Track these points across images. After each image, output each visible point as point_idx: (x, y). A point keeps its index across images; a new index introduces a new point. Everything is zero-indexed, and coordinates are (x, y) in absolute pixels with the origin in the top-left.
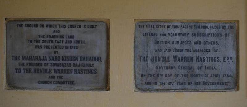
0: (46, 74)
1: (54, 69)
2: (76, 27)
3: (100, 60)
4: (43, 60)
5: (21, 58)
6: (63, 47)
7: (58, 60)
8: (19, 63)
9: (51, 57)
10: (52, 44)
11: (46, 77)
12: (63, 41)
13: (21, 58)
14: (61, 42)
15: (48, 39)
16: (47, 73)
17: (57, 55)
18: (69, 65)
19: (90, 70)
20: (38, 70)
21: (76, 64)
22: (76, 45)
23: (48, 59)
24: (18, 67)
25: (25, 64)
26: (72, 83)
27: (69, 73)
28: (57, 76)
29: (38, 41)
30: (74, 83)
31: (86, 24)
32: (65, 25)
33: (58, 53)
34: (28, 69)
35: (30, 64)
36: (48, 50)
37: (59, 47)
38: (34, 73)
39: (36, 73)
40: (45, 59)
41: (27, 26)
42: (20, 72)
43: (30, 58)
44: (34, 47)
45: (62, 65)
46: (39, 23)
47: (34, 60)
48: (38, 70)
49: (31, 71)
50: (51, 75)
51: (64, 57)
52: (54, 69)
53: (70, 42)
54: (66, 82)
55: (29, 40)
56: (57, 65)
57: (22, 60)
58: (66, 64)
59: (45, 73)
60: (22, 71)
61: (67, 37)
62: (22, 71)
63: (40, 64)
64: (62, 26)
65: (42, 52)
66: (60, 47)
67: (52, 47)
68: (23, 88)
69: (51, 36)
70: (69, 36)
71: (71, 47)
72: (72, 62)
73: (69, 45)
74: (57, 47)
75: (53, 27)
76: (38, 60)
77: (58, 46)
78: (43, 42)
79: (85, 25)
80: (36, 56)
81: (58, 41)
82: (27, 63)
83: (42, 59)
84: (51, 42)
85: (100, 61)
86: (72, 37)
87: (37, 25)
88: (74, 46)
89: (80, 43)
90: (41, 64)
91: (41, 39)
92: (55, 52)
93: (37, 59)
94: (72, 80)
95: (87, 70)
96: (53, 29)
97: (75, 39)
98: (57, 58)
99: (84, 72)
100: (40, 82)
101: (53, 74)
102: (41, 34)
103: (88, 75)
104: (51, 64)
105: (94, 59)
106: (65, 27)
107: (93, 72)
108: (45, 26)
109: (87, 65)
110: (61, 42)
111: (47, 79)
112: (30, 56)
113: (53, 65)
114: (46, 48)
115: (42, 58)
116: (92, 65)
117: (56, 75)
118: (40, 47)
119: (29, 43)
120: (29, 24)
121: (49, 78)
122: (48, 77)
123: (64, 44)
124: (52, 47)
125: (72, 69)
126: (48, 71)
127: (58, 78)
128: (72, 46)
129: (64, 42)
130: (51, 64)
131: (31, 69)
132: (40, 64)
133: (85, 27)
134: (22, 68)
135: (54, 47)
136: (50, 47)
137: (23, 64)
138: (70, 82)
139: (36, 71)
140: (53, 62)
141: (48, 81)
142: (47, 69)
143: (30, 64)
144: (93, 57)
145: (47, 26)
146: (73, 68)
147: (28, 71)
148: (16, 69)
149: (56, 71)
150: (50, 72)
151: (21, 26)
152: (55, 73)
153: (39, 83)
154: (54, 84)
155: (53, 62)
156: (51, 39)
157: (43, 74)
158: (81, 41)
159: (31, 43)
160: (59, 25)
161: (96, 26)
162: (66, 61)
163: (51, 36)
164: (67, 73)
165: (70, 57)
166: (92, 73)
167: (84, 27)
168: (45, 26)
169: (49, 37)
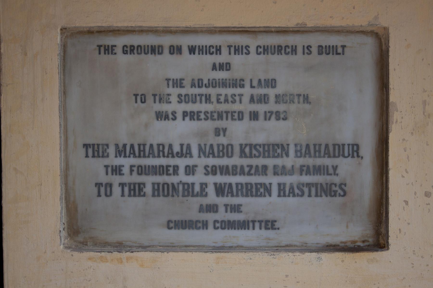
0: (190, 198)
1: (215, 184)
2: (283, 51)
3: (355, 154)
4: (180, 155)
5: (112, 150)
7: (228, 156)
8: (106, 167)
9: (205, 145)
10: (209, 107)
11: (190, 208)
12: (241, 95)
13: (112, 150)
14: (237, 98)
15: (196, 91)
16: (193, 196)
17: (223, 140)
18: (260, 169)
19: (325, 186)
20: (166, 186)
21: (284, 167)
22: (281, 107)
23: (195, 151)
24: (104, 179)
25: (126, 170)
26: (270, 226)
27: (261, 195)
28: (226, 206)
29: (162, 98)
30: (277, 225)
31: (315, 41)
32: (247, 47)
33: (227, 133)
34: (135, 184)
35: (142, 170)
37: (230, 115)
38: (153, 195)
39: (159, 195)
40: (185, 152)
41: (129, 50)
42: (108, 193)
43: (141, 150)
44: (154, 115)
45: (238, 170)
46: (167, 41)
47: (214, 156)
48: (166, 186)
49: (145, 190)
50: (206, 201)
51: (246, 145)
52: (215, 184)
53: (264, 99)
54: (254, 222)
55: (136, 95)
56: (225, 170)
57: (116, 157)
58: (251, 167)
59: (188, 195)
60: (117, 190)
61: (255, 83)
62: (117, 190)
63: (171, 170)
64: (237, 50)
65: (178, 132)
66: (232, 116)
67: (209, 115)
68: (120, 247)
69: (205, 82)
70: (260, 81)
71: (268, 115)
72: (270, 162)
73: (261, 108)
74: (224, 115)
75: (212, 54)
76: (164, 156)
77: (227, 113)
78: (181, 99)
79: (309, 47)
80: (159, 145)
81: (226, 95)
82: (131, 166)
83: (178, 153)
84: (203, 98)
85: (358, 156)
86: (271, 83)
87: (161, 47)
89: (296, 100)
90: (176, 168)
91: (175, 92)
92: (217, 132)
93: (161, 154)
94: (270, 217)
95: (317, 184)
96: (210, 59)
97: (280, 89)
98: (225, 151)
99: (306, 190)
100: (172, 225)
101: (212, 197)
102: (175, 75)
103: (319, 199)
104: (206, 167)
105: (338, 150)
106: (248, 53)
108: (185, 50)
110: (237, 98)
111: (194, 215)
112: (139, 145)
113: (212, 171)
114: (191, 120)
115: (177, 149)
116: (331, 171)
117: (221, 201)
118: (171, 116)
119: (136, 105)
120: (136, 44)
121: (201, 209)
122: (196, 207)
123: (246, 107)
125: (270, 184)
126: (197, 188)
127: (226, 211)
128: (271, 113)
129: (246, 99)
130: (206, 167)
131: (144, 184)
132: (171, 169)
133: (310, 53)
134: (116, 180)
135: (216, 116)
136: (202, 116)
137: (117, 170)
138: (263, 224)
139: (161, 190)
140: (211, 161)
141: (197, 221)
142: (193, 184)
143: (142, 170)
144: (334, 145)
145: (192, 50)
146: (274, 181)
147: (136, 190)
148: (98, 185)
149: (220, 190)
150: (203, 193)
151: (109, 50)
152: (218, 195)
153: (169, 228)
154: (215, 228)
155: (211, 161)
156: (203, 90)
157: (180, 197)
158: (299, 95)
159: (143, 105)
160: (230, 47)
161: (343, 47)
162: (251, 157)
163: (205, 82)
164: (256, 196)
165: (264, 145)
166: (331, 196)
167: (306, 51)
168: (185, 50)
169: (198, 83)
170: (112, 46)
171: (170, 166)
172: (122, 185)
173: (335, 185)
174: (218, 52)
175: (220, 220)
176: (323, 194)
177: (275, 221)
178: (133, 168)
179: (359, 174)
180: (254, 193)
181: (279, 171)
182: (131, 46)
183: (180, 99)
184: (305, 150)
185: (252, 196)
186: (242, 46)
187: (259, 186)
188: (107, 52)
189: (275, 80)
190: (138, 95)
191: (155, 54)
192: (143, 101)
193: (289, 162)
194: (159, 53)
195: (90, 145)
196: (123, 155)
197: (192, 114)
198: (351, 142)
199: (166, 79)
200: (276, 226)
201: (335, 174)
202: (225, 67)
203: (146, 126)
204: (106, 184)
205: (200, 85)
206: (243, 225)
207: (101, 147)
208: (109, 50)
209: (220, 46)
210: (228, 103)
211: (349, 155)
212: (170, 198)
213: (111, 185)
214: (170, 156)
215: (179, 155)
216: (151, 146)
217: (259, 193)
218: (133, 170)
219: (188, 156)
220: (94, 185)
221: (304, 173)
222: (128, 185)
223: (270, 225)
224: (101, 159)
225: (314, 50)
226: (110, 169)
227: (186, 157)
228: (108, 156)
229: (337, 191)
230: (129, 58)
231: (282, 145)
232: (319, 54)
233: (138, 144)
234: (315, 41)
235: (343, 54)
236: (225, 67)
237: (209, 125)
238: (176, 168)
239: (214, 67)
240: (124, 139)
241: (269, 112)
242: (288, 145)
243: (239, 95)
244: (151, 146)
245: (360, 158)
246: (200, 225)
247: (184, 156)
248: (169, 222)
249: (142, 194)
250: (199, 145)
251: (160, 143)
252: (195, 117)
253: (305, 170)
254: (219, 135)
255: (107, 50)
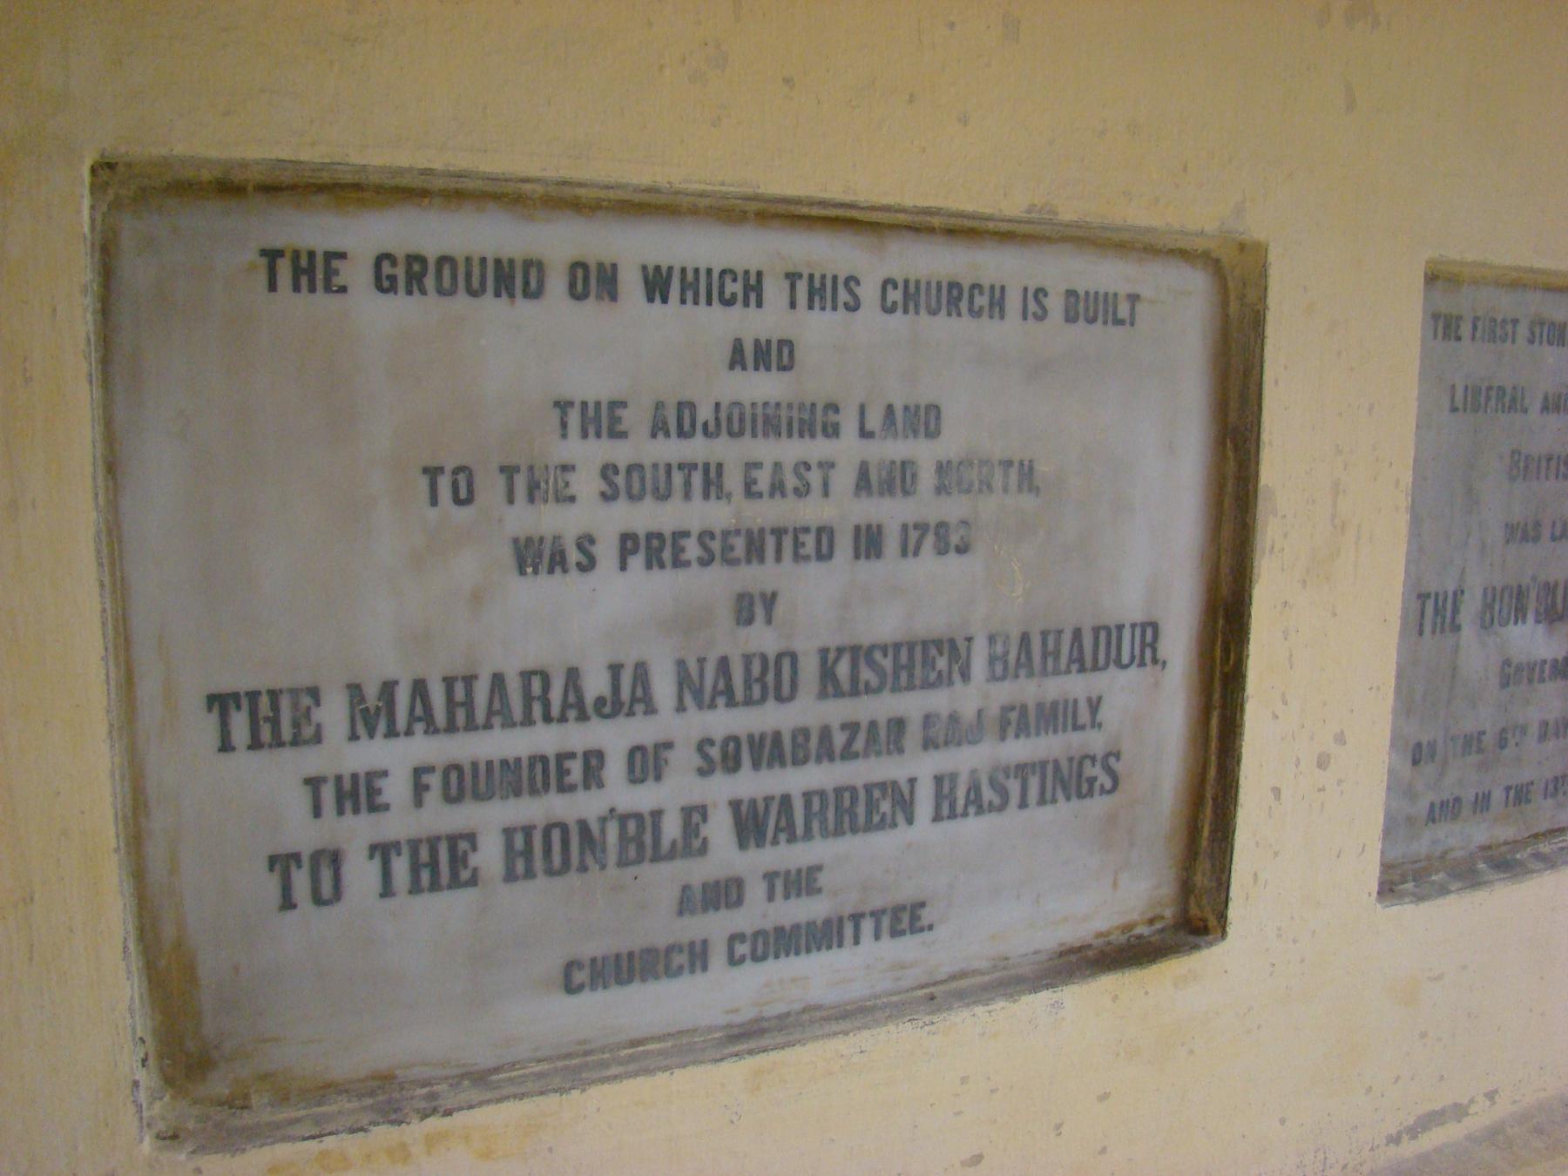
0: (647, 871)
1: (735, 805)
2: (964, 305)
4: (611, 707)
5: (333, 714)
6: (824, 543)
7: (780, 698)
8: (314, 783)
9: (701, 661)
10: (717, 515)
11: (647, 903)
12: (827, 466)
13: (333, 714)
15: (671, 450)
16: (657, 858)
17: (763, 639)
18: (883, 733)
19: (1064, 765)
20: (556, 835)
21: (954, 718)
22: (952, 509)
23: (664, 688)
24: (303, 834)
25: (396, 789)
26: (905, 924)
27: (882, 825)
28: (770, 877)
29: (538, 483)
30: (926, 916)
32: (852, 280)
34: (433, 842)
35: (463, 783)
36: (666, 582)
38: (510, 876)
39: (530, 874)
40: (628, 695)
41: (402, 274)
43: (457, 702)
44: (506, 554)
48: (556, 835)
49: (474, 860)
50: (698, 871)
51: (840, 651)
52: (735, 805)
53: (899, 479)
54: (856, 918)
55: (433, 473)
56: (770, 751)
57: (354, 737)
58: (852, 728)
60: (361, 874)
61: (874, 421)
64: (821, 291)
65: (602, 616)
66: (797, 544)
67: (716, 546)
70: (890, 409)
71: (913, 535)
72: (912, 705)
73: (890, 512)
75: (728, 302)
76: (547, 718)
77: (779, 533)
78: (618, 483)
79: (1040, 292)
80: (527, 676)
81: (777, 466)
82: (419, 772)
83: (600, 701)
84: (697, 479)
85: (1155, 661)
86: (925, 420)
87: (534, 266)
88: (932, 520)
89: (998, 481)
90: (594, 761)
91: (588, 454)
92: (747, 608)
93: (537, 710)
97: (949, 445)
98: (770, 678)
101: (724, 854)
102: (591, 384)
103: (1048, 812)
104: (703, 745)
106: (853, 307)
107: (1092, 781)
108: (631, 284)
109: (1053, 716)
110: (815, 477)
111: (662, 927)
112: (449, 682)
113: (726, 756)
114: (649, 566)
115: (596, 684)
118: (574, 556)
119: (432, 513)
120: (431, 251)
121: (685, 905)
122: (668, 897)
123: (842, 509)
124: (716, 549)
126: (671, 828)
127: (771, 897)
128: (922, 528)
129: (844, 479)
131: (471, 838)
133: (1042, 316)
135: (739, 543)
136: (692, 550)
137: (359, 793)
139: (534, 853)
140: (723, 722)
142: (657, 814)
143: (463, 783)
144: (1096, 630)
145: (657, 284)
147: (441, 864)
148: (282, 863)
149: (751, 824)
150: (692, 843)
151: (314, 271)
152: (742, 844)
153: (571, 988)
154: (734, 961)
155: (723, 722)
157: (612, 870)
158: (1008, 464)
159: (464, 513)
160: (792, 277)
161: (1134, 298)
162: (855, 692)
163: (705, 413)
164: (869, 827)
165: (897, 646)
166: (1080, 796)
168: (631, 284)
169: (678, 419)
170: (331, 256)
171: (572, 755)
172: (383, 851)
173: (1093, 759)
174: (753, 297)
175: (748, 929)
176: (1060, 795)
177: (923, 905)
178: (426, 779)
179: (1152, 714)
180: (862, 819)
181: (943, 733)
182: (412, 259)
183: (611, 484)
184: (1028, 652)
185: (854, 830)
186: (835, 278)
187: (877, 794)
188: (304, 280)
189: (937, 407)
190: (441, 470)
191: (512, 296)
192: (463, 494)
193: (972, 696)
194: (527, 294)
195: (235, 696)
196: (382, 727)
197: (655, 543)
198: (1138, 617)
199: (557, 404)
200: (925, 922)
201: (1093, 726)
202: (772, 355)
203: (477, 598)
204: (316, 857)
205: (687, 427)
206: (825, 935)
207: (285, 703)
208: (314, 271)
209: (759, 274)
210: (783, 495)
211: (1133, 658)
212: (573, 878)
213: (336, 858)
214: (572, 714)
215: (607, 709)
216: (498, 680)
217: (876, 819)
218: (427, 788)
219: (639, 708)
220: (263, 864)
221: (1011, 731)
222: (405, 850)
223: (906, 918)
224: (287, 754)
225: (1055, 304)
226: (328, 794)
227: (631, 714)
228: (318, 738)
229: (1095, 779)
230: (401, 308)
231: (952, 641)
232: (1068, 320)
233: (445, 679)
234: (1060, 271)
235: (1132, 324)
236: (772, 355)
237: (714, 585)
238: (594, 761)
239: (737, 358)
240: (385, 661)
241: (916, 527)
242: (969, 639)
243: (820, 465)
244: (498, 680)
245: (1159, 667)
246: (680, 959)
247: (625, 709)
248: (571, 966)
249: (465, 875)
250: (681, 664)
251: (530, 664)
252: (667, 555)
253: (1015, 721)
254: (750, 621)
255: (304, 271)
